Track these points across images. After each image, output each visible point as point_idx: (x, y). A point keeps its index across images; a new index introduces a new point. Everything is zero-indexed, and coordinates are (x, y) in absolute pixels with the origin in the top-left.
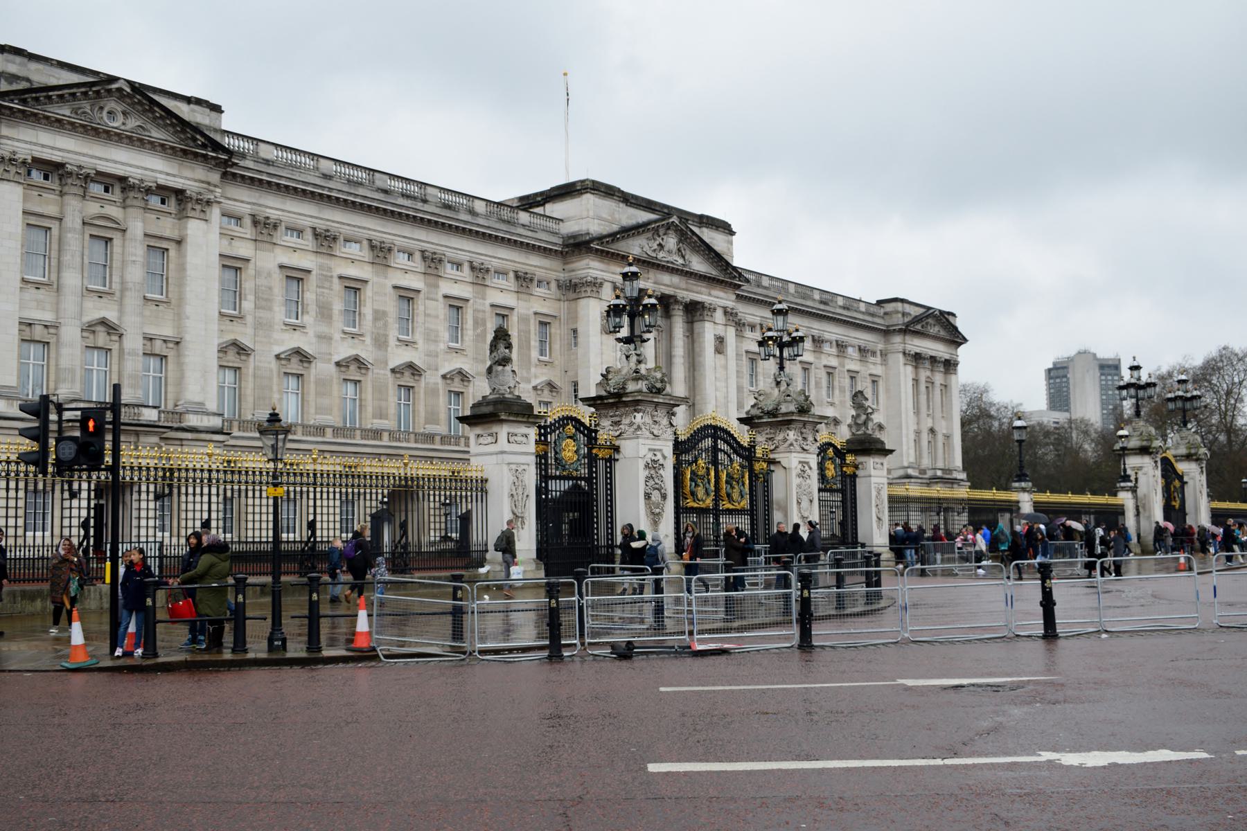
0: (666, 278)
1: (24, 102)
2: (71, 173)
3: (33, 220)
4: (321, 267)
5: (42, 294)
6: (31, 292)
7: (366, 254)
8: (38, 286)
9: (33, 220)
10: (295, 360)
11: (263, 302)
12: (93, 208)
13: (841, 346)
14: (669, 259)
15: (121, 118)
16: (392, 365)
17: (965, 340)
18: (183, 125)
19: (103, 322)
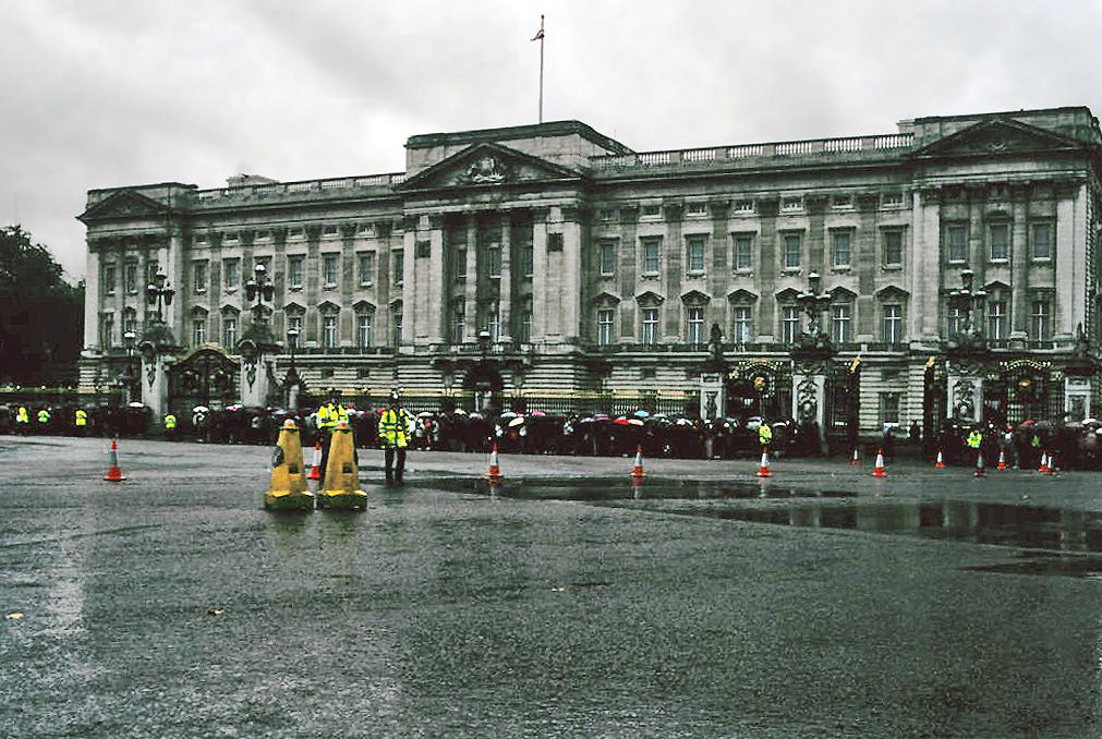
0: (486, 197)
6: (108, 301)
11: (216, 281)
12: (129, 253)
13: (816, 206)
14: (486, 178)
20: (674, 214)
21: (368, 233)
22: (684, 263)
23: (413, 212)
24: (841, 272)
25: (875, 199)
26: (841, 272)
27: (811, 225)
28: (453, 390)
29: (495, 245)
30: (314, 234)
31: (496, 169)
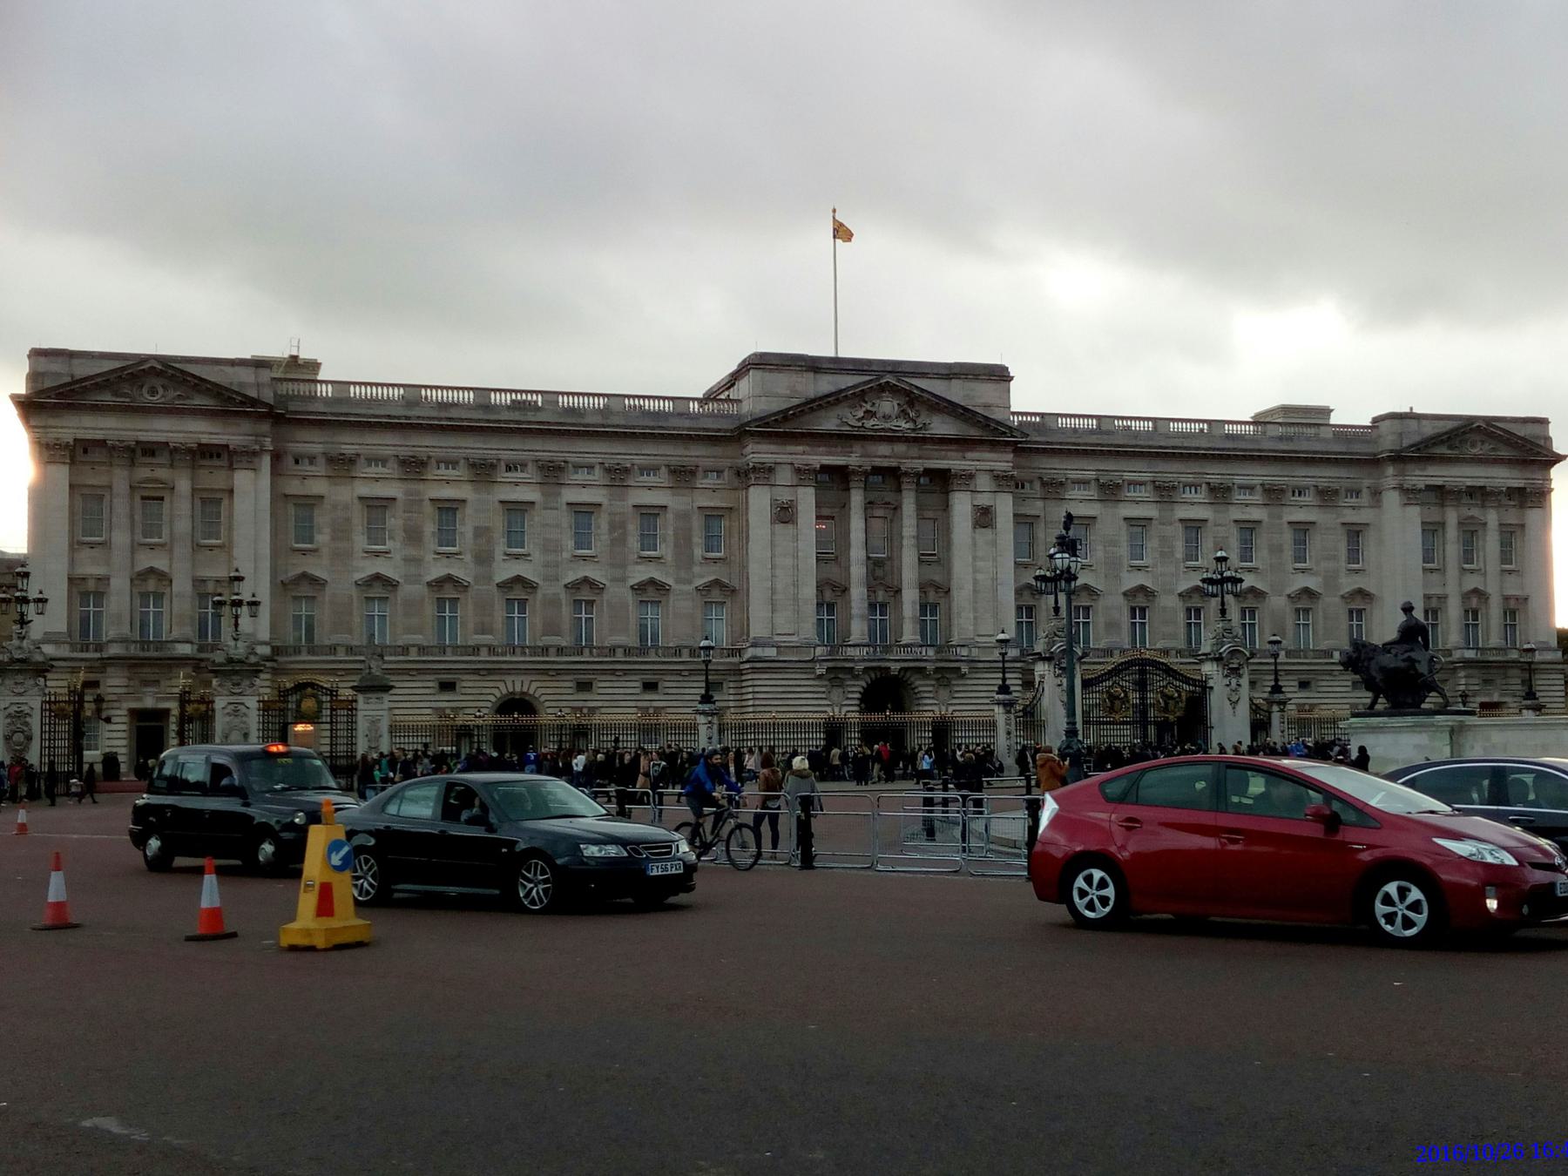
0: (884, 449)
1: (59, 395)
2: (114, 447)
3: (86, 491)
4: (407, 493)
5: (95, 552)
6: (86, 553)
7: (461, 472)
8: (92, 545)
9: (86, 491)
10: (377, 584)
11: (341, 532)
13: (1274, 494)
14: (887, 426)
15: (161, 391)
16: (499, 579)
17: (1564, 457)
18: (217, 391)
19: (152, 570)
20: (1110, 491)
21: (651, 479)
22: (1124, 550)
23: (768, 458)
24: (1303, 571)
25: (1336, 492)
26: (1303, 571)
27: (1270, 516)
28: (845, 709)
29: (879, 513)
30: (552, 472)
31: (903, 414)
